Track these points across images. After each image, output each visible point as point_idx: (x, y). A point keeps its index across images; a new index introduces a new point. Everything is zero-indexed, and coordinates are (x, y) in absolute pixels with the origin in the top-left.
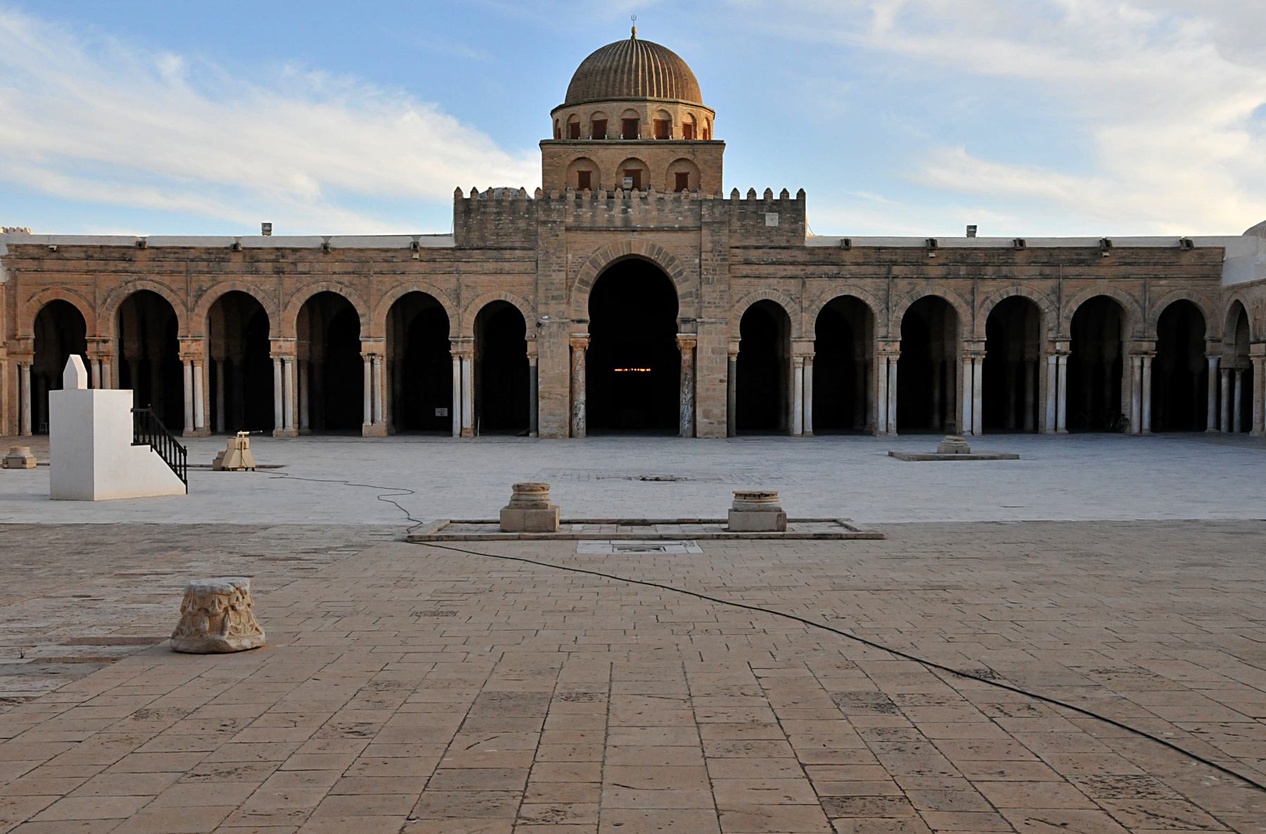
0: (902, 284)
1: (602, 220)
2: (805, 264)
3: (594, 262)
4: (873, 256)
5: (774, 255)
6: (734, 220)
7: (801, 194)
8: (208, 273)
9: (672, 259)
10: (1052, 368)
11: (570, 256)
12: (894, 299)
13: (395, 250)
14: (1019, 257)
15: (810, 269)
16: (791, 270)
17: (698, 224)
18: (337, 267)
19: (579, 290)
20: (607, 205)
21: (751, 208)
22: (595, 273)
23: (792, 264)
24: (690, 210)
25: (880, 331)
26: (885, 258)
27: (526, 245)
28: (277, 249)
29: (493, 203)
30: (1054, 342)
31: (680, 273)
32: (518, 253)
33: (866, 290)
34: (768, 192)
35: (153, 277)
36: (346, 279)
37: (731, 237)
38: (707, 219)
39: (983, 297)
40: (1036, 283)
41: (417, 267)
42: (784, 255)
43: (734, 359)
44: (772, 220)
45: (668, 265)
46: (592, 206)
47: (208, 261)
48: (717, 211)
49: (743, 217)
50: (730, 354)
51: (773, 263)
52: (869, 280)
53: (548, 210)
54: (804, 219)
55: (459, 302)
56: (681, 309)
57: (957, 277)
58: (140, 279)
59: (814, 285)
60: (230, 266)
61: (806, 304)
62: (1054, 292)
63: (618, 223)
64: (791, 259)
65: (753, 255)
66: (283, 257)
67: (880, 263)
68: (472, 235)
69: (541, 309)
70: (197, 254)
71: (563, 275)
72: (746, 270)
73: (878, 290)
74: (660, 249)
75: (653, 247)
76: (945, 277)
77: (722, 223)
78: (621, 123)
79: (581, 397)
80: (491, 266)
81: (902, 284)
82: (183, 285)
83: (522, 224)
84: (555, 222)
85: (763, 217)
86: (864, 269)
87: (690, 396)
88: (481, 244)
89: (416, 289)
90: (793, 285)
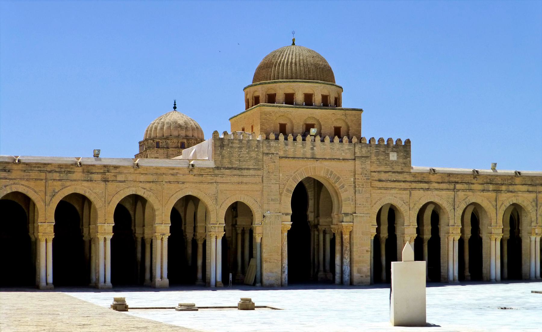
0: (461, 194)
1: (299, 154)
2: (411, 182)
3: (294, 179)
4: (447, 179)
5: (395, 177)
6: (373, 156)
7: (408, 142)
8: (60, 180)
9: (338, 178)
10: (533, 243)
11: (281, 175)
12: (457, 203)
13: (179, 169)
14: (518, 180)
15: (414, 185)
16: (403, 185)
17: (353, 158)
18: (142, 178)
20: (303, 144)
21: (382, 149)
22: (295, 185)
23: (404, 181)
24: (349, 149)
25: (451, 222)
26: (452, 180)
27: (256, 167)
28: (105, 166)
29: (237, 141)
30: (535, 229)
31: (343, 187)
32: (252, 172)
33: (441, 197)
34: (390, 140)
35: (23, 182)
36: (148, 186)
37: (371, 166)
38: (358, 154)
39: (501, 203)
40: (526, 195)
41: (191, 178)
42: (400, 177)
43: (373, 238)
44: (393, 156)
45: (336, 182)
46: (294, 145)
47: (60, 172)
48: (364, 150)
49: (377, 154)
51: (394, 181)
52: (444, 192)
54: (410, 157)
55: (217, 202)
57: (489, 191)
58: (14, 184)
59: (416, 194)
60: (74, 176)
61: (411, 206)
62: (534, 201)
63: (309, 156)
64: (403, 180)
65: (383, 176)
66: (108, 171)
67: (450, 182)
68: (225, 160)
69: (265, 207)
70: (53, 168)
71: (278, 185)
72: (380, 184)
73: (449, 198)
74: (332, 172)
75: (328, 170)
76: (483, 191)
77: (367, 157)
78: (303, 96)
79: (286, 262)
80: (236, 179)
82: (43, 189)
83: (253, 154)
84: (273, 154)
85: (388, 155)
87: (349, 260)
88: (230, 166)
89: (190, 193)
90: (405, 195)
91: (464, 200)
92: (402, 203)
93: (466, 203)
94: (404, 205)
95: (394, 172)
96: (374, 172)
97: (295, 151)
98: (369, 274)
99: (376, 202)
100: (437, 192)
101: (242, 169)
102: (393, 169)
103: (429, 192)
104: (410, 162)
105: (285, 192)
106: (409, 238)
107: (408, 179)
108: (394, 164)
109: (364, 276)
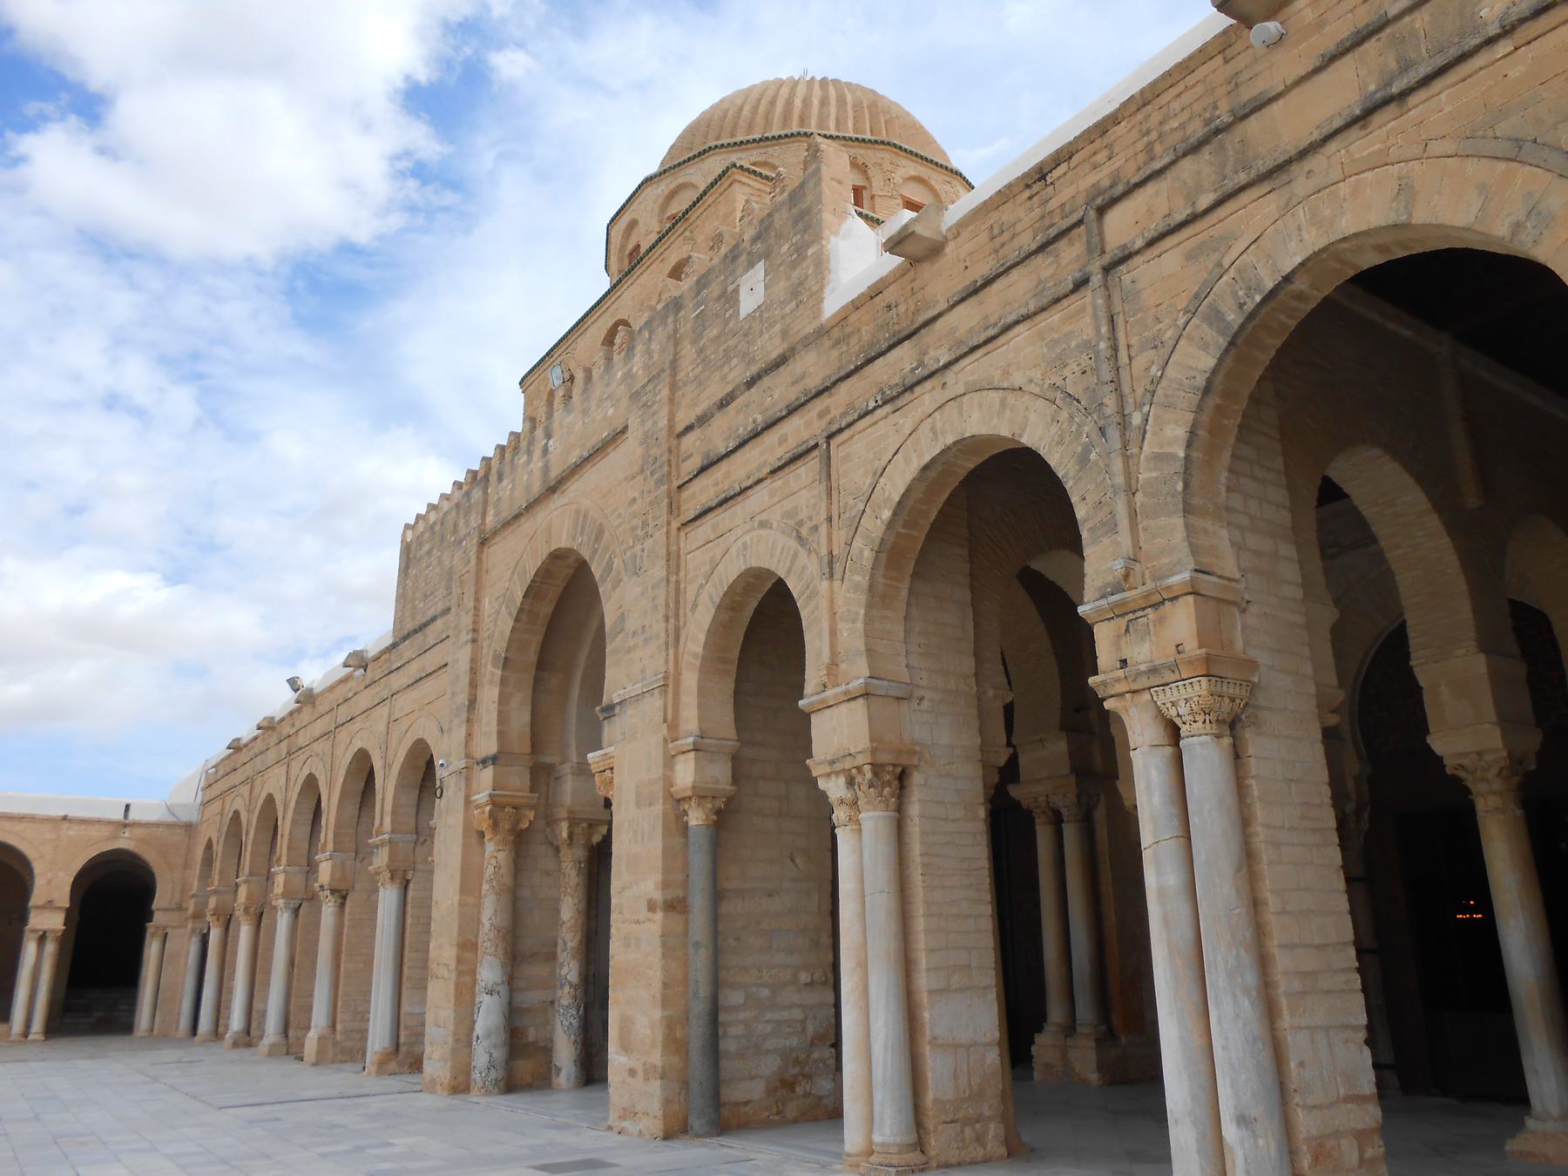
4: (1025, 223)
9: (599, 537)
16: (799, 430)
19: (491, 682)
23: (792, 410)
31: (609, 568)
42: (779, 390)
43: (696, 817)
50: (677, 803)
51: (756, 435)
53: (467, 513)
56: (608, 674)
59: (858, 455)
65: (719, 434)
71: (469, 647)
72: (704, 491)
73: (1061, 362)
81: (1162, 278)
86: (995, 302)
91: (1198, 298)
92: (793, 544)
93: (1215, 317)
94: (803, 554)
95: (751, 383)
96: (689, 428)
97: (513, 489)
98: (656, 1057)
99: (698, 595)
100: (970, 370)
101: (426, 625)
102: (752, 361)
103: (928, 396)
104: (821, 266)
105: (489, 667)
106: (842, 780)
107: (813, 383)
108: (757, 326)
109: (640, 1074)
